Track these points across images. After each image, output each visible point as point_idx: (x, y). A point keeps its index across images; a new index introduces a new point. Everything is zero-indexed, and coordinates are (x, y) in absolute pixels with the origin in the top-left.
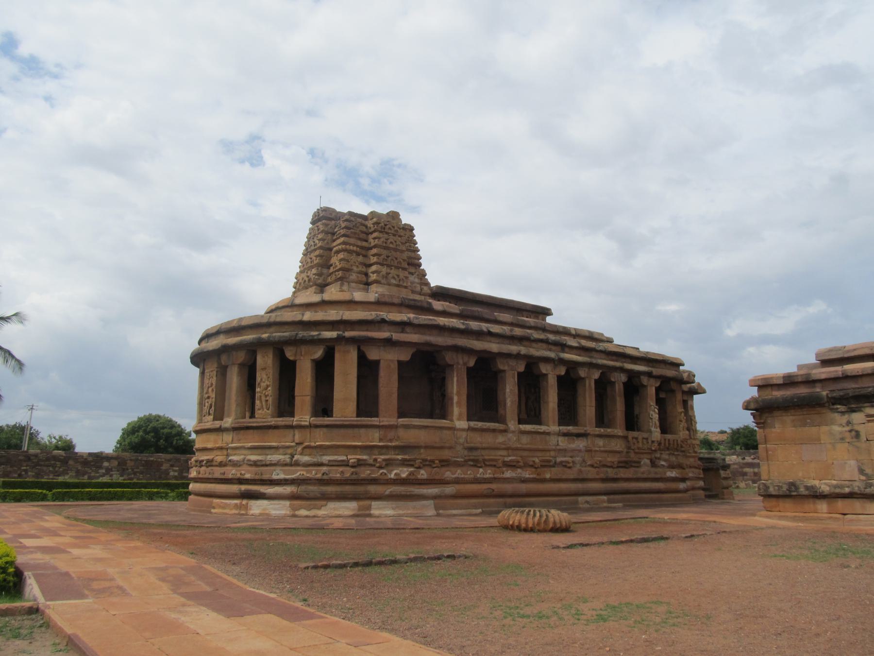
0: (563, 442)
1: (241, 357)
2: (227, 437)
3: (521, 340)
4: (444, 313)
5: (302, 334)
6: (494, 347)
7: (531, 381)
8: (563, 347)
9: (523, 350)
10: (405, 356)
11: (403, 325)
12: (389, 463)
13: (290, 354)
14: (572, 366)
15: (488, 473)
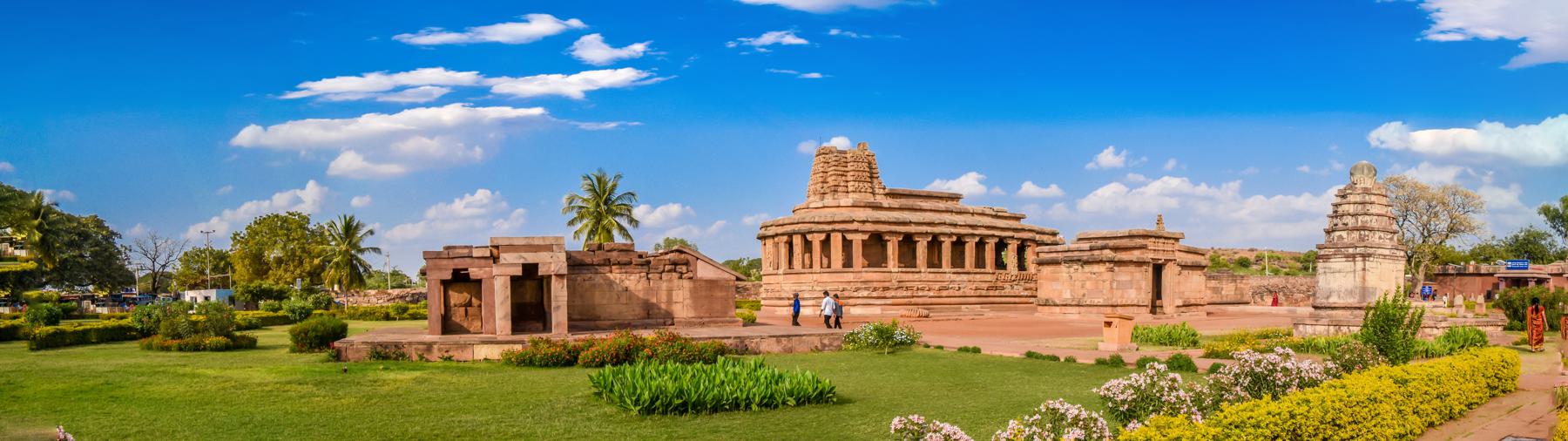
0: (954, 277)
1: (785, 238)
2: (781, 278)
3: (929, 224)
4: (890, 209)
5: (815, 227)
6: (912, 229)
7: (935, 243)
8: (955, 225)
9: (929, 229)
10: (866, 237)
11: (864, 222)
12: (857, 290)
13: (809, 237)
14: (960, 236)
15: (909, 293)
